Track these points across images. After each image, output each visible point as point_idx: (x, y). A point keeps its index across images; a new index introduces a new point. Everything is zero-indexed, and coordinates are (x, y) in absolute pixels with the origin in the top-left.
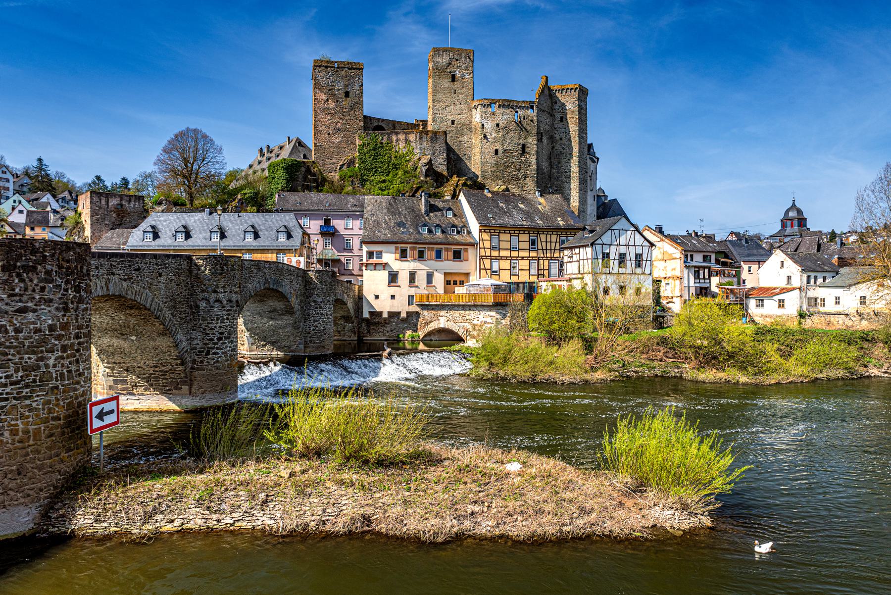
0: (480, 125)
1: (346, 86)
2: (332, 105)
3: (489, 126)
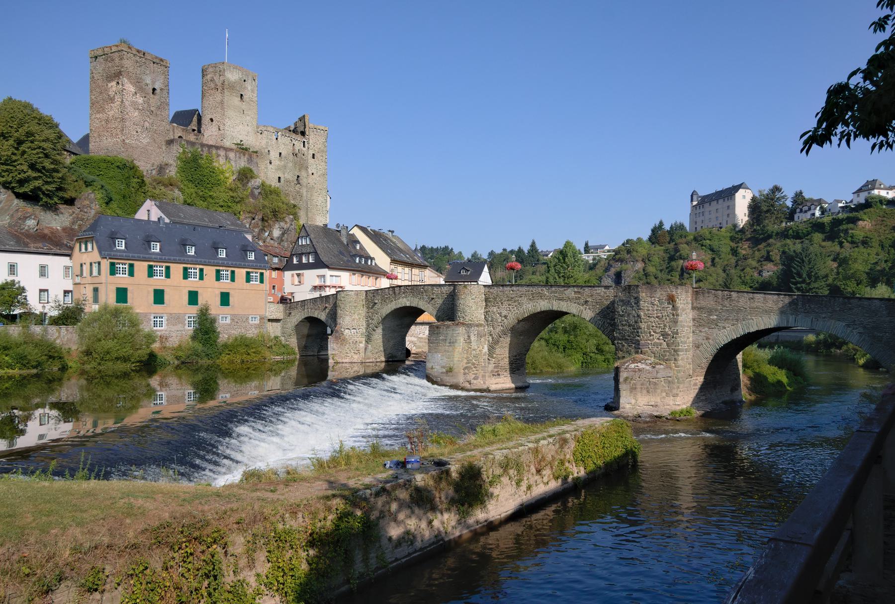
0: (266, 151)
1: (153, 83)
2: (141, 100)
3: (274, 155)
